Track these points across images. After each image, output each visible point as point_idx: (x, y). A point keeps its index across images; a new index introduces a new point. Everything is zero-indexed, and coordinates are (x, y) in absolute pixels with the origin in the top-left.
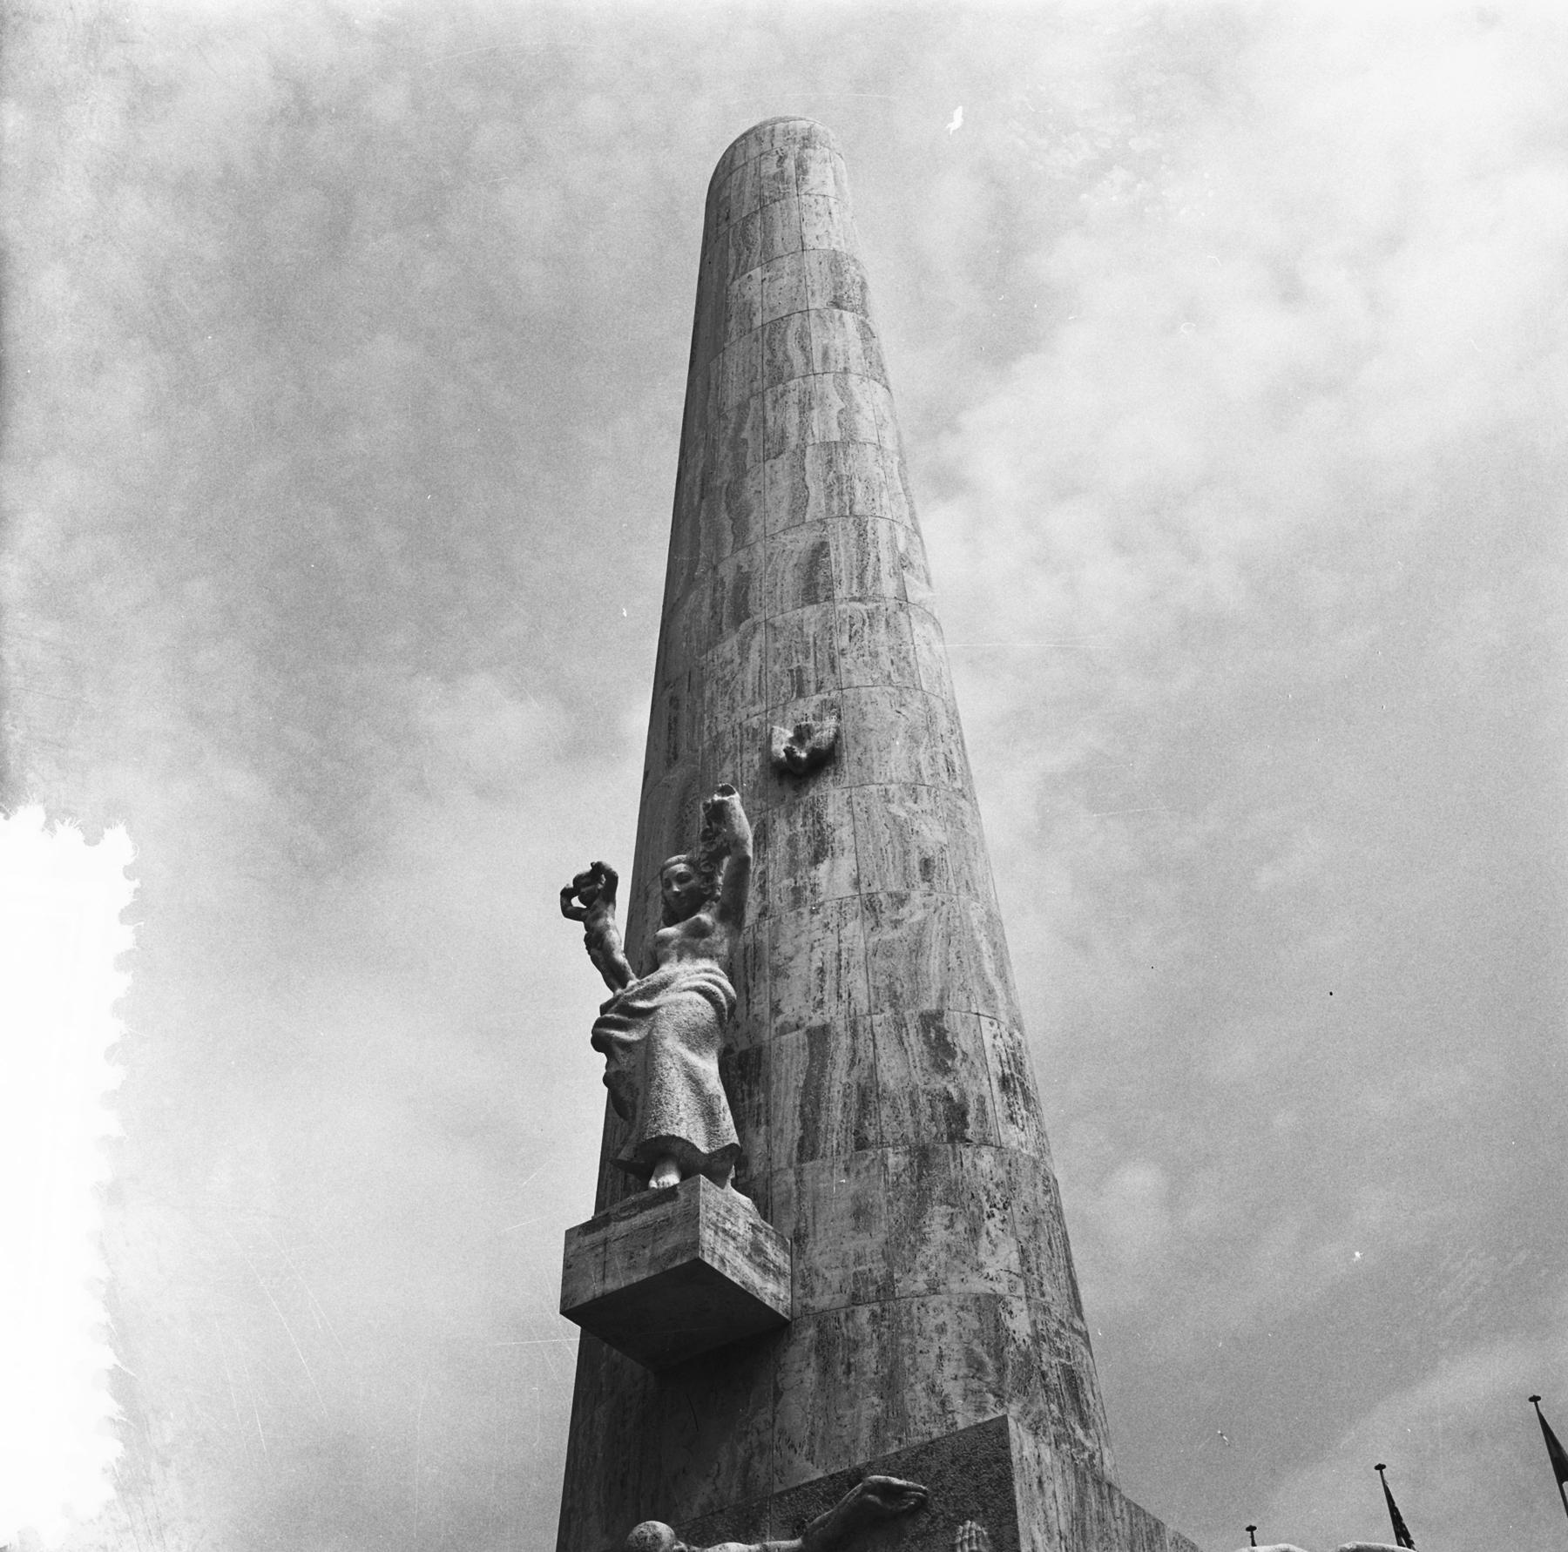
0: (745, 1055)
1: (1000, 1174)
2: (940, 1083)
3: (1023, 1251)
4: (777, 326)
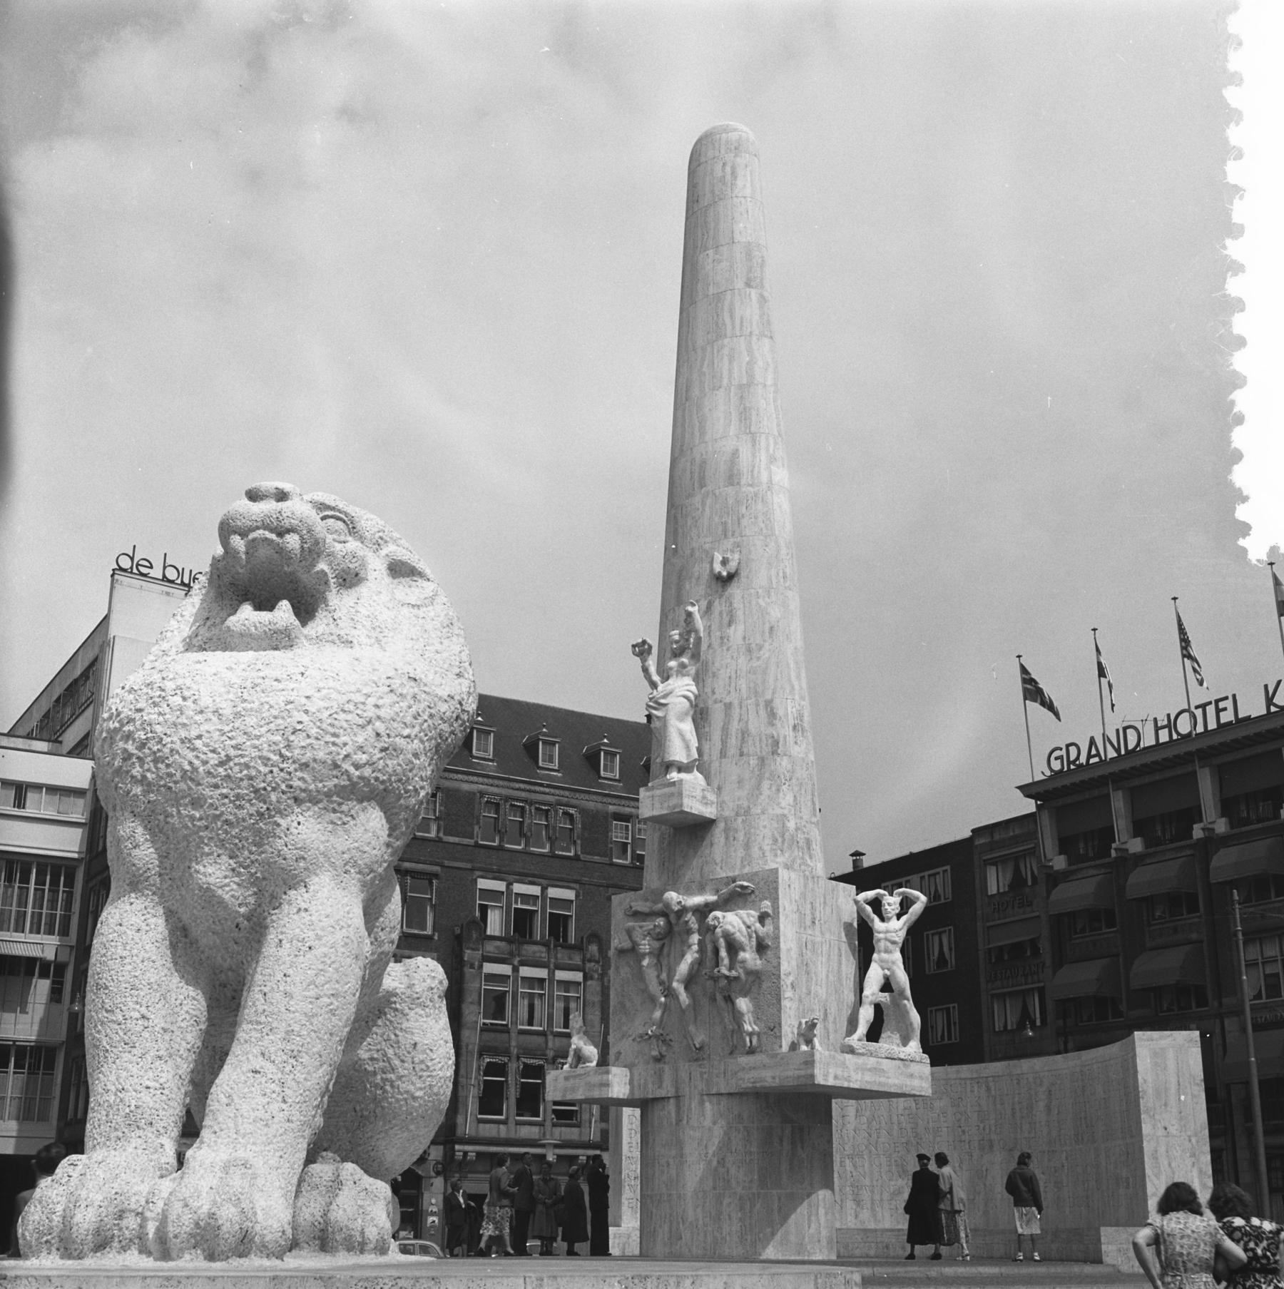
1: (789, 767)
4: (719, 297)
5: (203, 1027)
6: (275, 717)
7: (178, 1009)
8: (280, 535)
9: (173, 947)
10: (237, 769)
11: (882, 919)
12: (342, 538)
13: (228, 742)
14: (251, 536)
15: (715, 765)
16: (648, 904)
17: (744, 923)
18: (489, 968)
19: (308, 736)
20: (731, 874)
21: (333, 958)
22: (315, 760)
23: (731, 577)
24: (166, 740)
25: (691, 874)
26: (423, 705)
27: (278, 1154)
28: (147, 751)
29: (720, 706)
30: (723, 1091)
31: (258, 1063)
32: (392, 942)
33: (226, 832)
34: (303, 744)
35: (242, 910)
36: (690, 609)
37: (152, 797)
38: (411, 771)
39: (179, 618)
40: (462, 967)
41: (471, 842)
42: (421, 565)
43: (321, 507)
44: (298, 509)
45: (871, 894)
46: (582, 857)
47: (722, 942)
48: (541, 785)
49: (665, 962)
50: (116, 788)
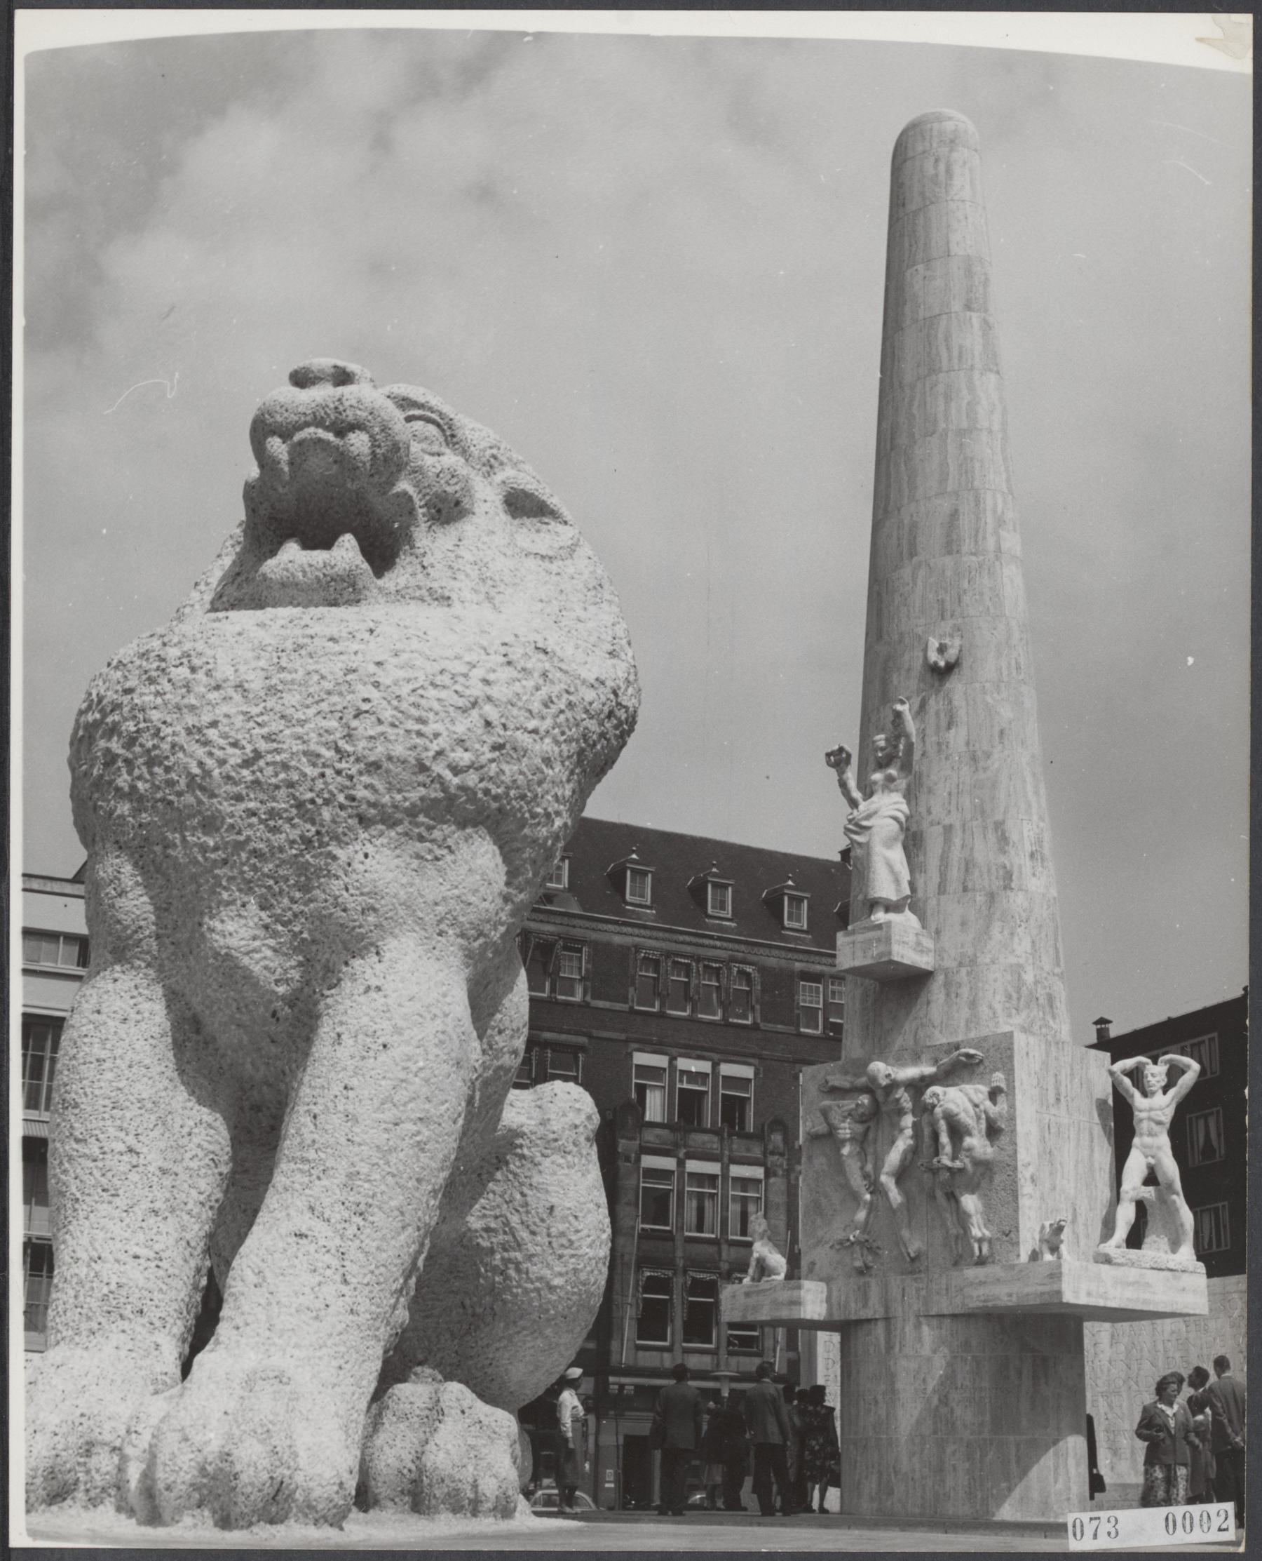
0: (915, 834)
1: (1026, 905)
2: (1002, 859)
3: (1033, 942)
5: (225, 1169)
6: (329, 693)
7: (185, 1141)
8: (340, 433)
9: (179, 1047)
10: (269, 771)
11: (1145, 1094)
12: (435, 448)
13: (258, 731)
14: (298, 437)
15: (933, 902)
16: (849, 1078)
17: (971, 1101)
18: (649, 1161)
19: (380, 721)
20: (953, 1039)
21: (421, 1064)
22: (390, 758)
23: (950, 668)
24: (166, 731)
25: (901, 1040)
26: (556, 689)
27: (335, 1363)
28: (137, 749)
29: (939, 829)
30: (946, 1312)
31: (305, 1222)
32: (515, 1052)
33: (255, 869)
34: (371, 733)
35: (281, 990)
36: (899, 707)
37: (145, 817)
38: (540, 783)
39: (202, 587)
41: (625, 1007)
42: (554, 501)
43: (404, 403)
44: (365, 395)
45: (1129, 1063)
46: (762, 1026)
47: (943, 1125)
48: (711, 937)
49: (870, 1150)
50: (95, 808)
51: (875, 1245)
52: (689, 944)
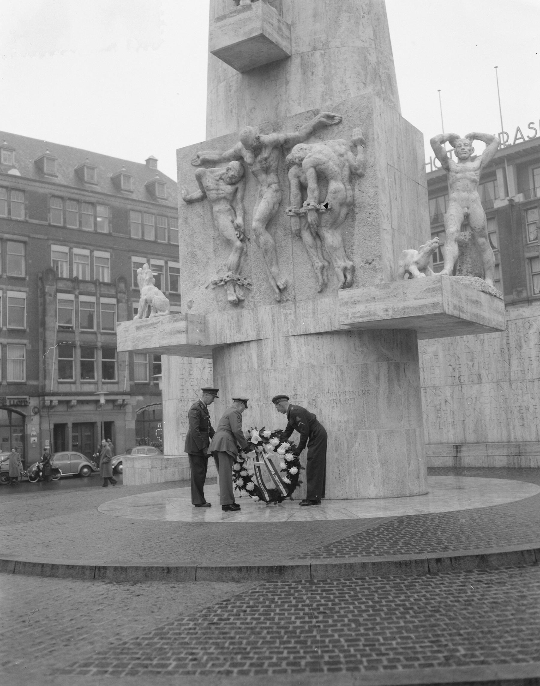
3: (374, 31)
16: (217, 152)
18: (60, 296)
40: (44, 295)
46: (114, 234)
49: (239, 207)
51: (246, 282)
52: (76, 194)
